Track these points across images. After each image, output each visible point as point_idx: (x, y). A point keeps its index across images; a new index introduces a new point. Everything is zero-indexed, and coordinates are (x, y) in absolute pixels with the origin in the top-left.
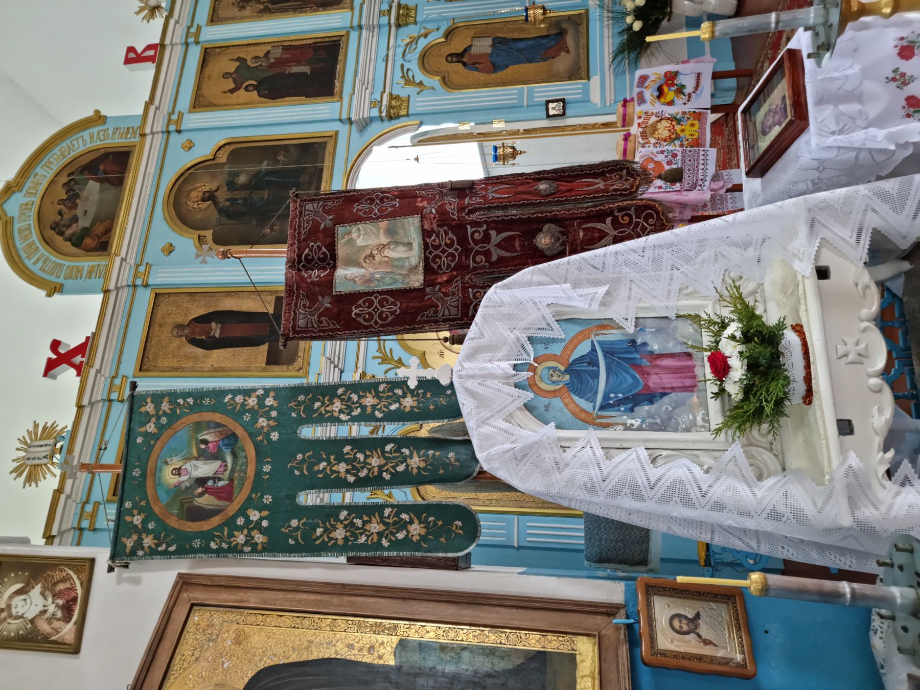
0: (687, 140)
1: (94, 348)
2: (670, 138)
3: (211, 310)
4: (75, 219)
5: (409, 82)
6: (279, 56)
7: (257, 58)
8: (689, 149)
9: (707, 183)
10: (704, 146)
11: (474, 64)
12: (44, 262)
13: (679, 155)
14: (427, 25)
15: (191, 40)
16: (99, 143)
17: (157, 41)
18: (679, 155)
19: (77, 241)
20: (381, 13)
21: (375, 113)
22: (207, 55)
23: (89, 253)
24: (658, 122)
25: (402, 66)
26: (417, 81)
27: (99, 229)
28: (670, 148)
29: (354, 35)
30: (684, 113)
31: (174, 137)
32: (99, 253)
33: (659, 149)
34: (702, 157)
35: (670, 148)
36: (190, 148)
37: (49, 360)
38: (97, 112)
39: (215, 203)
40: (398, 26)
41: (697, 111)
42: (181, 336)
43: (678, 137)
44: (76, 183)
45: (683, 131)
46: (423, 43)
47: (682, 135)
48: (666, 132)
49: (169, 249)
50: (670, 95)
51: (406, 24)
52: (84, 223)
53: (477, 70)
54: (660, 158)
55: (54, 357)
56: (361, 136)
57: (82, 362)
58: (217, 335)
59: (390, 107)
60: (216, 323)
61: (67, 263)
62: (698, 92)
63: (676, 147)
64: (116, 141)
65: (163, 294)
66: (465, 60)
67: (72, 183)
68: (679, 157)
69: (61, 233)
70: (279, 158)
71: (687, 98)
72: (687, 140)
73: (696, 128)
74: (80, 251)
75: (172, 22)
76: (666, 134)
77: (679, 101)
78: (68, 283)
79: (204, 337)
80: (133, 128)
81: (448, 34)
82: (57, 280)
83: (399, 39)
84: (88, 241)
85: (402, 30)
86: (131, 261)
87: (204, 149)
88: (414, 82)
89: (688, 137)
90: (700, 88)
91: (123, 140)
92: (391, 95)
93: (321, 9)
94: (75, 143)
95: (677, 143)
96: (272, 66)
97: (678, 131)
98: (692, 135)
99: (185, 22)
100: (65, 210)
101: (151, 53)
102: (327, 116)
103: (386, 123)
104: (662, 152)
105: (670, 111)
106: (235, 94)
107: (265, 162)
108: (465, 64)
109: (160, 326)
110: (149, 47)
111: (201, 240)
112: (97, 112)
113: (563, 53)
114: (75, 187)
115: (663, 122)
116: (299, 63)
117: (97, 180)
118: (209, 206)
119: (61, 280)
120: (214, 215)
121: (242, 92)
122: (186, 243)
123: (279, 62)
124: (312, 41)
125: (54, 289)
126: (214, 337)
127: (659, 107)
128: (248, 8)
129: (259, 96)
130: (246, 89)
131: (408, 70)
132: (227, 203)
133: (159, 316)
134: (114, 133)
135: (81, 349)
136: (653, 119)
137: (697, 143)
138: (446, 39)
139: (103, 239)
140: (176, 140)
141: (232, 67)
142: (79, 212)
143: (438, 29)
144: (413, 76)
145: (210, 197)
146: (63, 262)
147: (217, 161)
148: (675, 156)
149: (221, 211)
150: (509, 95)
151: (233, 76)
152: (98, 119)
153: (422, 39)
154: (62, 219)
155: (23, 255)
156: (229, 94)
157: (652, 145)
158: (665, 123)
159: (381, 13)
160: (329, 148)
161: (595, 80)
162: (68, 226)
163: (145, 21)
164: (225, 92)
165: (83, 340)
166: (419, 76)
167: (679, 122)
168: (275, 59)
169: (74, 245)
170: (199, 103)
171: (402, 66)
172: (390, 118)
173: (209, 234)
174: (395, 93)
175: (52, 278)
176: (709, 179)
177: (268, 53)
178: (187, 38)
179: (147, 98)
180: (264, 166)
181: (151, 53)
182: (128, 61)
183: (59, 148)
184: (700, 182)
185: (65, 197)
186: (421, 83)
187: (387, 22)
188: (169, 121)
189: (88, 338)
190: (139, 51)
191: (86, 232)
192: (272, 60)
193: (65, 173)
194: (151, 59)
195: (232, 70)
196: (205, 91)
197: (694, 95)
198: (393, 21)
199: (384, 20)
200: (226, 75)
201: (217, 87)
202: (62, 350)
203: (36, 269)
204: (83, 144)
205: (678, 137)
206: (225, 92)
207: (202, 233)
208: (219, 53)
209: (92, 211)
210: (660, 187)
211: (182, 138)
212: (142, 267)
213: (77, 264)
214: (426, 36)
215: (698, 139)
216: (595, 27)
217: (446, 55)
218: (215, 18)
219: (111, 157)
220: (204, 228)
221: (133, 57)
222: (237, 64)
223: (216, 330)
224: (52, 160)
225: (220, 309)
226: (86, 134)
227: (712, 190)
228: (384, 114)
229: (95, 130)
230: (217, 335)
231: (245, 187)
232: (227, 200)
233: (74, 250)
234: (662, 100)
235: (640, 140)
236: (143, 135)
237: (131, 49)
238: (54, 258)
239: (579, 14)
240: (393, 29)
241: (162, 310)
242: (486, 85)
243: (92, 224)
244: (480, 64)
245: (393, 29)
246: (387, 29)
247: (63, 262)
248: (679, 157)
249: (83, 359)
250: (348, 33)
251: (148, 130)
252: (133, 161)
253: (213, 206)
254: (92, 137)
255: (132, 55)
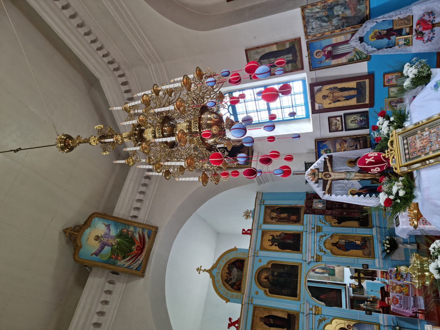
0: (405, 293)
1: (240, 322)
2: (400, 292)
3: (270, 314)
4: (231, 279)
5: (321, 250)
6: (283, 236)
7: (277, 236)
8: (405, 296)
9: (411, 308)
10: (410, 296)
11: (340, 247)
12: (224, 291)
13: (403, 297)
14: (325, 233)
15: (259, 228)
16: (236, 256)
17: (251, 228)
18: (403, 297)
19: (232, 286)
20: (312, 228)
21: (312, 260)
22: (264, 233)
23: (236, 291)
24: (396, 285)
25: (319, 245)
26: (324, 251)
27: (238, 283)
28: (400, 295)
29: (304, 233)
30: (403, 284)
31: (256, 257)
32: (238, 291)
33: (396, 294)
34: (409, 299)
35: (400, 295)
36: (261, 262)
37: (229, 323)
38: (235, 247)
39: (269, 280)
40: (317, 232)
41: (407, 284)
42: (262, 321)
43: (402, 292)
44: (231, 268)
45: (403, 290)
46: (324, 238)
47: (403, 291)
48: (398, 289)
49: (257, 293)
50: (399, 278)
51: (319, 232)
52: (234, 281)
53: (341, 249)
54: (397, 297)
55: (230, 323)
56: (308, 266)
57: (237, 326)
58: (272, 323)
59: (317, 258)
60: (272, 319)
61: (230, 293)
62: (407, 278)
63: (401, 295)
64: (240, 256)
65: (256, 307)
66: (337, 246)
67: (230, 268)
68: (403, 298)
69: (228, 283)
70: (285, 269)
71: (404, 279)
72: (405, 293)
73: (407, 289)
74: (233, 290)
75: (254, 223)
76: (398, 290)
77: (402, 280)
78: (231, 299)
79: (268, 323)
80: (245, 253)
81: (332, 237)
82: (228, 298)
83: (318, 236)
84: (235, 287)
85: (318, 233)
86: (247, 295)
87: (264, 263)
88: (323, 251)
89: (405, 292)
90: (407, 277)
91: (242, 256)
92: (316, 254)
93: (294, 223)
94: (229, 255)
95: (402, 294)
96: (282, 239)
97: (402, 290)
98: (406, 292)
99: (257, 222)
100: (228, 276)
101: (249, 232)
102: (298, 258)
103: (315, 263)
104: (398, 296)
105: (399, 283)
106: (272, 246)
107: (282, 269)
108: (337, 247)
109: (256, 317)
110: (249, 230)
111: (265, 291)
112: (235, 247)
113: (366, 248)
114: (230, 269)
115: (398, 286)
116: (289, 240)
117: (236, 268)
118: (267, 281)
119: (229, 298)
120: (269, 284)
121: (274, 246)
122: (261, 291)
123: (284, 238)
124: (292, 233)
125: (228, 301)
126: (271, 323)
127: (395, 281)
128: (274, 220)
129: (279, 248)
130: (275, 245)
131: (321, 246)
132: (272, 281)
133: (256, 314)
134: (240, 254)
135: (237, 322)
136: (395, 285)
137: (408, 295)
138: (331, 238)
139: (239, 287)
140: (257, 259)
141: (271, 238)
142: (232, 277)
143: (329, 234)
144: (322, 249)
145: (266, 278)
146: (229, 292)
147: (268, 267)
148: (401, 297)
149: (271, 283)
150: (351, 260)
151: (271, 241)
152: (235, 249)
153: (324, 237)
154: (227, 279)
155: (218, 289)
156: (270, 246)
157: (395, 293)
158: (398, 287)
159: (312, 228)
160: (299, 267)
161: (377, 260)
162: (230, 281)
163: (246, 219)
164: (269, 245)
165: (237, 319)
166: (324, 249)
167: (402, 287)
168: (283, 237)
169: (231, 287)
170: (262, 248)
171: (319, 245)
172: (316, 261)
173: (267, 290)
174: (318, 254)
175: (226, 297)
176: (411, 307)
177: (280, 234)
178: (258, 227)
179: (249, 246)
180: (282, 270)
181: (249, 232)
182: (243, 233)
183: (225, 256)
184: (409, 308)
185: (228, 272)
186: (325, 252)
187: (314, 231)
188: (255, 253)
189: (238, 319)
190: (246, 230)
191: (234, 283)
192: (282, 237)
193: (227, 264)
194: (249, 234)
195: (271, 239)
196: (264, 244)
197: (406, 279)
198: (316, 231)
199: (313, 230)
200: (269, 240)
201: (267, 244)
202: (233, 321)
203: (222, 293)
204: (232, 256)
205: (402, 292)
206: (269, 245)
207: (266, 289)
208: (267, 233)
209: (236, 277)
210: (398, 307)
211: (259, 258)
212: (251, 299)
213: (233, 294)
214: (325, 236)
215: (408, 294)
216: (376, 241)
217: (331, 243)
218: (265, 222)
219: (239, 261)
220: (266, 288)
221: (245, 232)
222: (272, 237)
223: (272, 321)
224: (224, 259)
225: (272, 315)
226: (232, 253)
227: (412, 310)
228: (315, 261)
229: (235, 252)
230: (272, 323)
231: (276, 276)
232: (272, 280)
233: (231, 289)
234: (397, 279)
235: (391, 290)
236: (249, 257)
237: (244, 230)
238: (227, 291)
239: (371, 236)
240: (316, 233)
241: (256, 312)
242: (344, 255)
243: (236, 282)
244: (342, 248)
245: (316, 233)
246: (314, 233)
247: (229, 292)
248: (403, 298)
249: (238, 325)
250: (303, 232)
251: (250, 256)
252: (246, 263)
253: (268, 281)
254: (234, 254)
255: (244, 232)
